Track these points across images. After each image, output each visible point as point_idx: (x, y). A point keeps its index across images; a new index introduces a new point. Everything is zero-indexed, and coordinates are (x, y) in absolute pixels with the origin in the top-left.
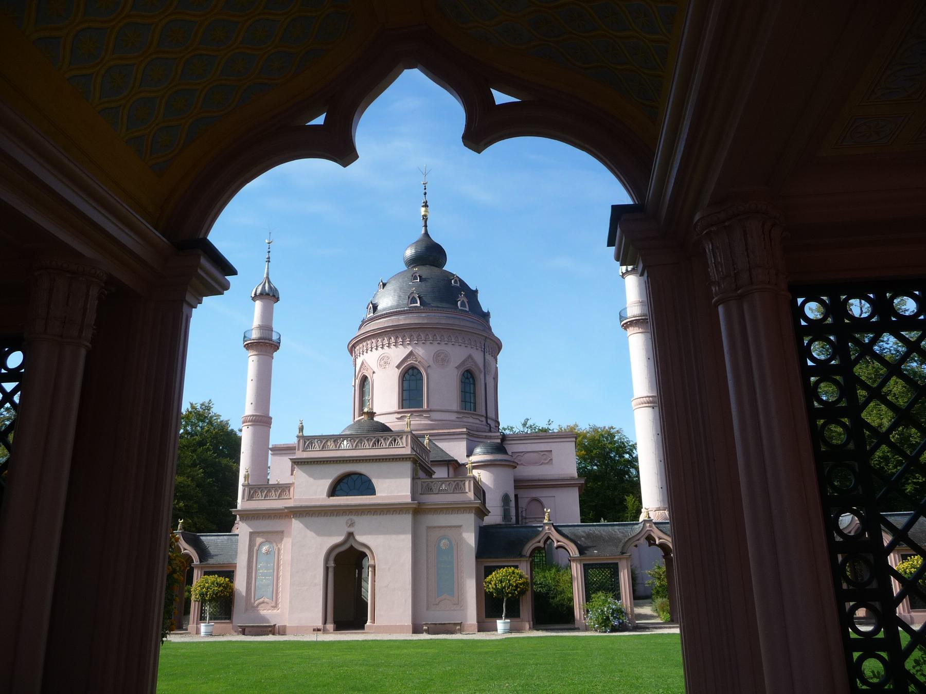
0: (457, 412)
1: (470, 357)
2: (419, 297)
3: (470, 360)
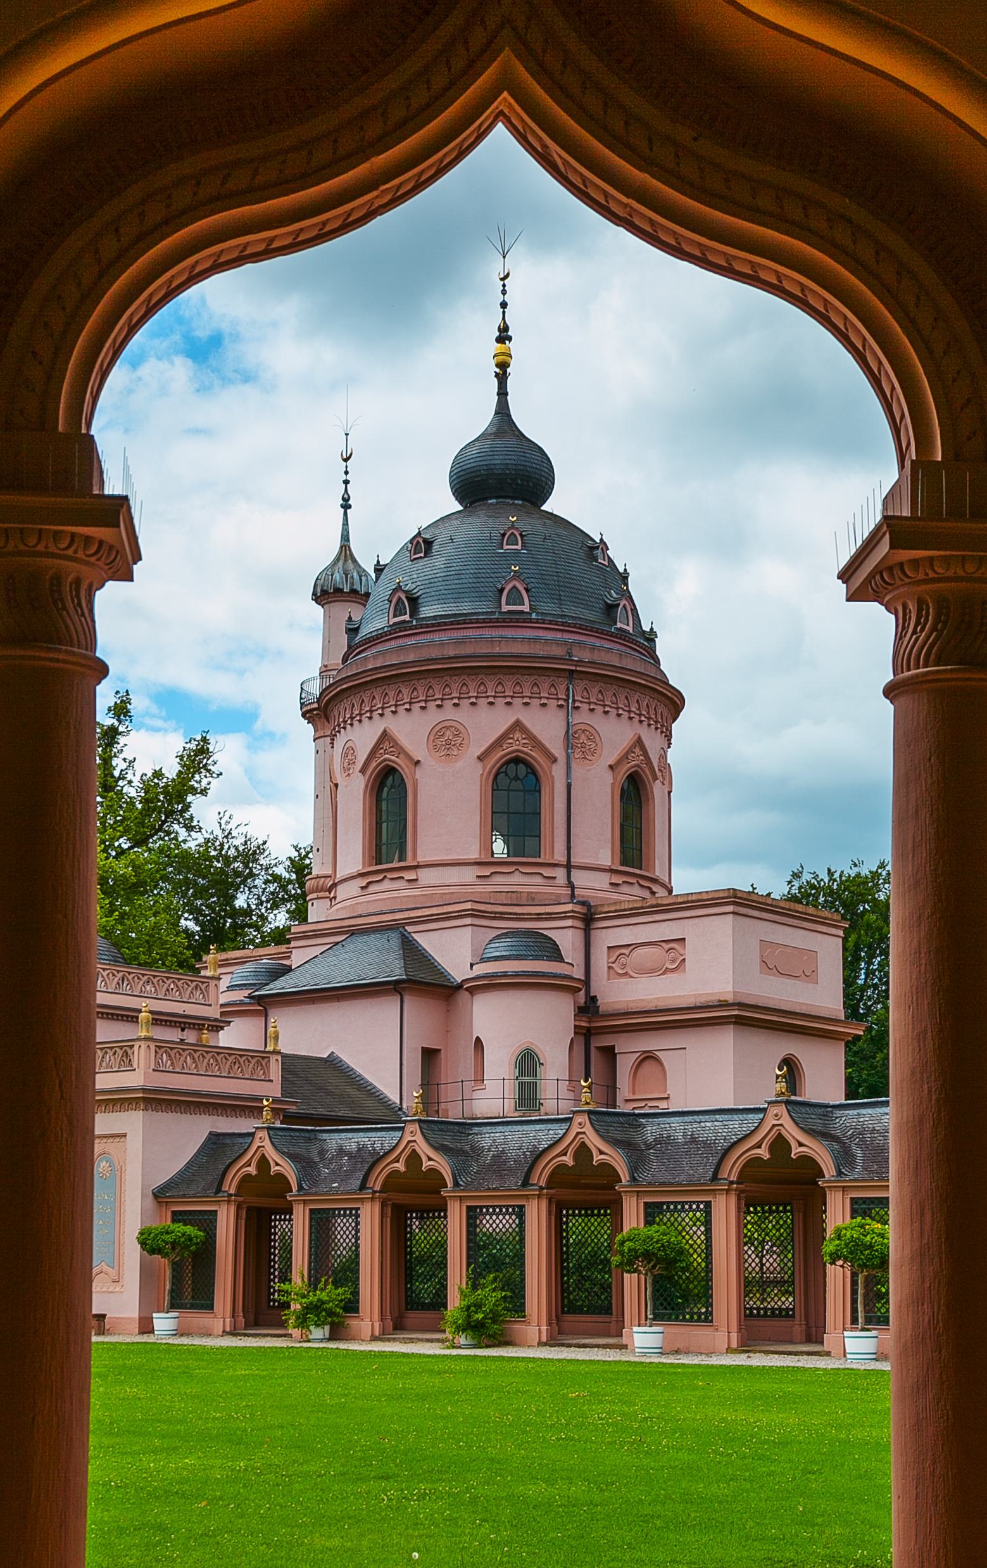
0: (612, 871)
1: (639, 742)
2: (527, 590)
3: (637, 750)
